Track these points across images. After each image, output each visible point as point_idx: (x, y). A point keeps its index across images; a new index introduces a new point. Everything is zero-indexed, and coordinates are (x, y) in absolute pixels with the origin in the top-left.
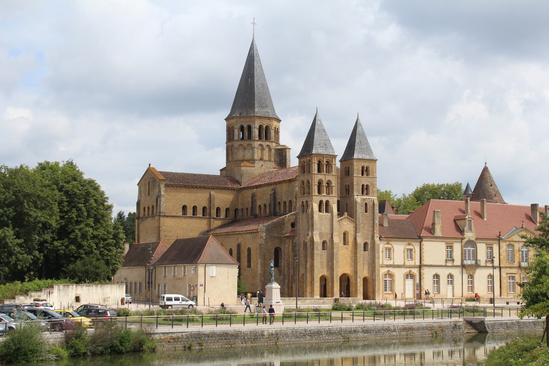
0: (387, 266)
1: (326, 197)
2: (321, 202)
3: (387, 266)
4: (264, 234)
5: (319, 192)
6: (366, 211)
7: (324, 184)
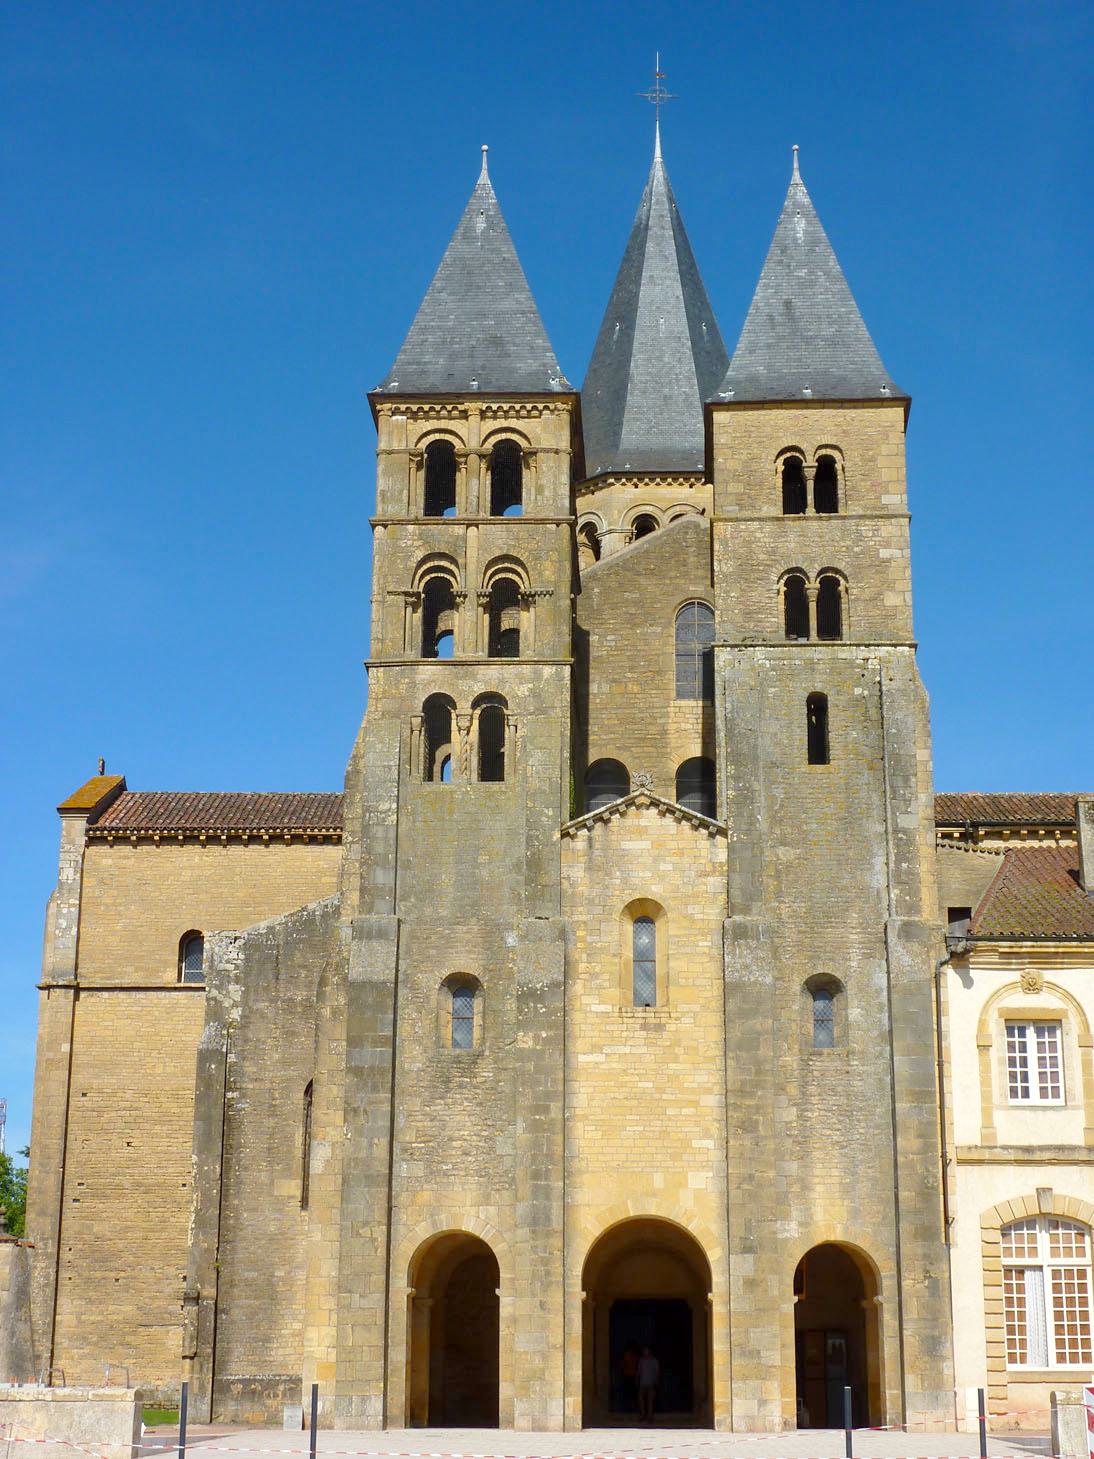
0: (1027, 1156)
1: (481, 670)
2: (437, 713)
3: (1027, 1156)
4: (235, 991)
5: (431, 641)
6: (818, 751)
7: (471, 580)
